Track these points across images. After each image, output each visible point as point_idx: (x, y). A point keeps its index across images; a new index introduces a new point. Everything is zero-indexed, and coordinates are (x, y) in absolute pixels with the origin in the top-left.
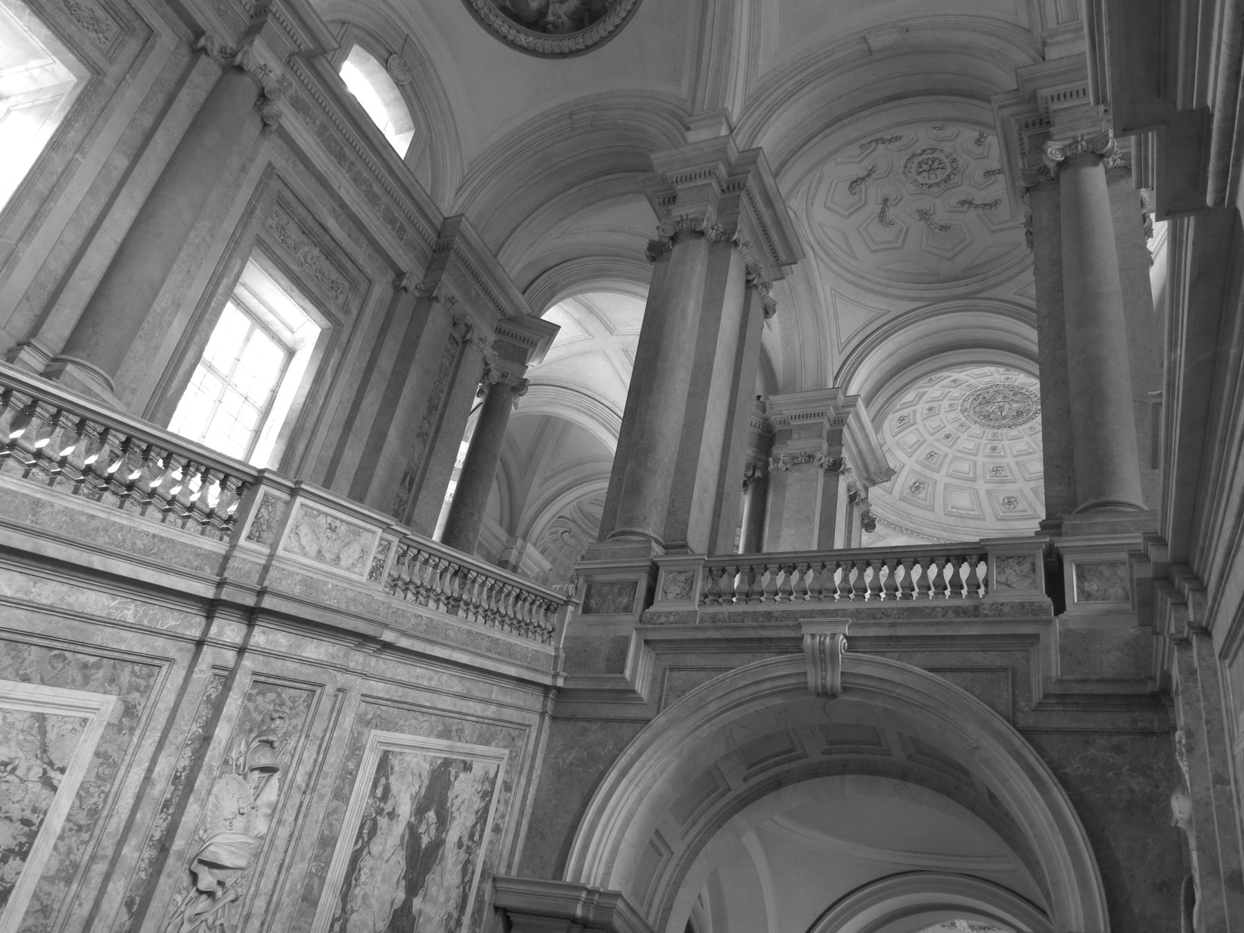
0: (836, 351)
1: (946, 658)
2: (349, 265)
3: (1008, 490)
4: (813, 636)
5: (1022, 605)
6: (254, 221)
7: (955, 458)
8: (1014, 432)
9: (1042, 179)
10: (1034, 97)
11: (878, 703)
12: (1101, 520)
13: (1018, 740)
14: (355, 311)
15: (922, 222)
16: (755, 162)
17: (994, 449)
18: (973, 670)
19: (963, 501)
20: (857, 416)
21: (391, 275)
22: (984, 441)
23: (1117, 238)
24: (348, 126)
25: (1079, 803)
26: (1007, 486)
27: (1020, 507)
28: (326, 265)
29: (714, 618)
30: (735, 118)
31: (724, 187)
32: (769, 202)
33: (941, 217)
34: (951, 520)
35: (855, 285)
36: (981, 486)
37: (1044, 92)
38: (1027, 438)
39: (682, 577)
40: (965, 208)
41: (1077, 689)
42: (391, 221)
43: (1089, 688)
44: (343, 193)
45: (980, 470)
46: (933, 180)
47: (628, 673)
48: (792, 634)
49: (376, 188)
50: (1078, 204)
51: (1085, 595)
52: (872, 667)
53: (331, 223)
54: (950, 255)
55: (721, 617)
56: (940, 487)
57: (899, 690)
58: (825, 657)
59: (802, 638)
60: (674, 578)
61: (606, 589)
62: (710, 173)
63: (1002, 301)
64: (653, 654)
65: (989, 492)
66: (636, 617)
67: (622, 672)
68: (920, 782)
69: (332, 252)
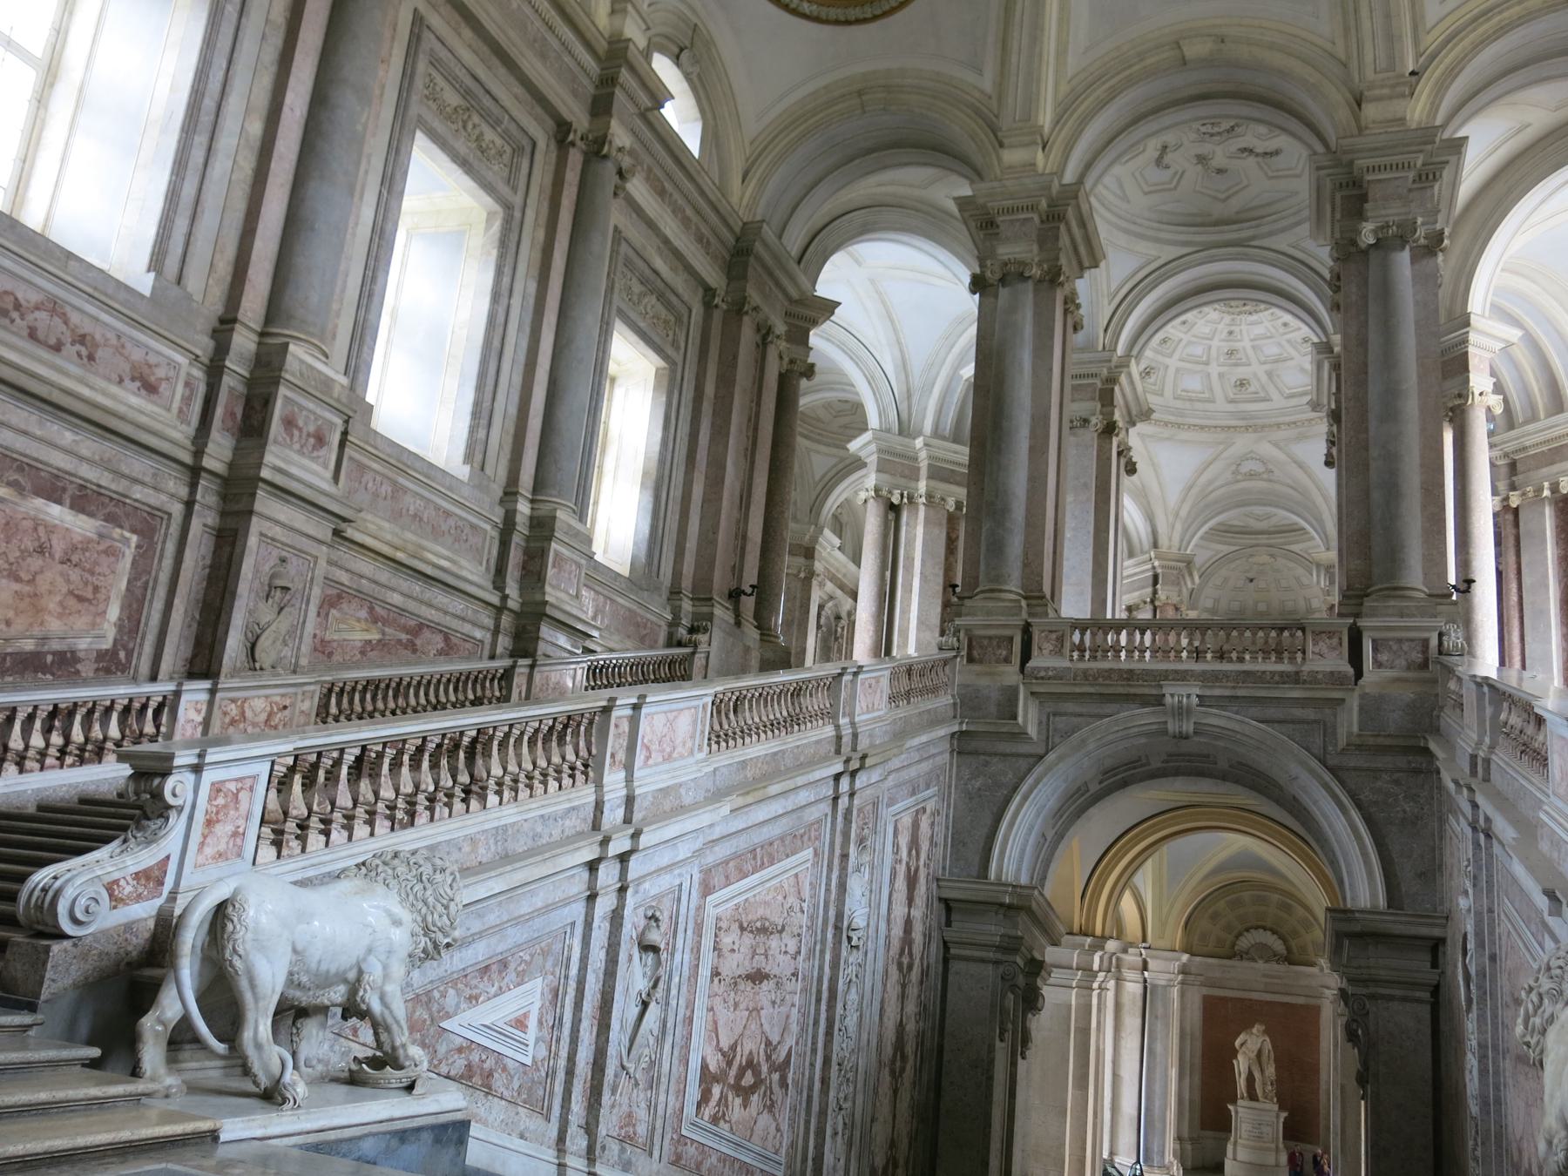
0: (1106, 302)
1: (1272, 712)
2: (674, 299)
3: (1241, 372)
4: (1172, 695)
5: (1332, 673)
6: (616, 297)
7: (1189, 343)
8: (1255, 317)
9: (1353, 249)
10: (1351, 163)
11: (1221, 743)
12: (1392, 603)
13: (1327, 777)
14: (683, 345)
16: (1076, 197)
17: (1231, 333)
18: (1293, 722)
19: (1194, 384)
20: (1130, 375)
21: (701, 291)
22: (1221, 326)
23: (1417, 323)
24: (669, 162)
25: (1369, 820)
26: (1240, 369)
27: (1252, 389)
28: (659, 306)
29: (1085, 672)
30: (1046, 130)
32: (1083, 224)
33: (1219, 160)
34: (1179, 404)
35: (1126, 231)
36: (1214, 370)
37: (1361, 163)
39: (1054, 636)
41: (1371, 741)
42: (700, 239)
43: (1380, 741)
44: (668, 232)
45: (1214, 352)
46: (1216, 129)
47: (1020, 720)
48: (1154, 692)
49: (689, 212)
50: (1387, 291)
51: (1378, 664)
52: (1217, 719)
53: (659, 264)
54: (1223, 196)
56: (1171, 371)
58: (1181, 712)
61: (986, 642)
62: (1033, 208)
65: (1221, 375)
67: (1015, 718)
68: (1237, 782)
69: (663, 292)
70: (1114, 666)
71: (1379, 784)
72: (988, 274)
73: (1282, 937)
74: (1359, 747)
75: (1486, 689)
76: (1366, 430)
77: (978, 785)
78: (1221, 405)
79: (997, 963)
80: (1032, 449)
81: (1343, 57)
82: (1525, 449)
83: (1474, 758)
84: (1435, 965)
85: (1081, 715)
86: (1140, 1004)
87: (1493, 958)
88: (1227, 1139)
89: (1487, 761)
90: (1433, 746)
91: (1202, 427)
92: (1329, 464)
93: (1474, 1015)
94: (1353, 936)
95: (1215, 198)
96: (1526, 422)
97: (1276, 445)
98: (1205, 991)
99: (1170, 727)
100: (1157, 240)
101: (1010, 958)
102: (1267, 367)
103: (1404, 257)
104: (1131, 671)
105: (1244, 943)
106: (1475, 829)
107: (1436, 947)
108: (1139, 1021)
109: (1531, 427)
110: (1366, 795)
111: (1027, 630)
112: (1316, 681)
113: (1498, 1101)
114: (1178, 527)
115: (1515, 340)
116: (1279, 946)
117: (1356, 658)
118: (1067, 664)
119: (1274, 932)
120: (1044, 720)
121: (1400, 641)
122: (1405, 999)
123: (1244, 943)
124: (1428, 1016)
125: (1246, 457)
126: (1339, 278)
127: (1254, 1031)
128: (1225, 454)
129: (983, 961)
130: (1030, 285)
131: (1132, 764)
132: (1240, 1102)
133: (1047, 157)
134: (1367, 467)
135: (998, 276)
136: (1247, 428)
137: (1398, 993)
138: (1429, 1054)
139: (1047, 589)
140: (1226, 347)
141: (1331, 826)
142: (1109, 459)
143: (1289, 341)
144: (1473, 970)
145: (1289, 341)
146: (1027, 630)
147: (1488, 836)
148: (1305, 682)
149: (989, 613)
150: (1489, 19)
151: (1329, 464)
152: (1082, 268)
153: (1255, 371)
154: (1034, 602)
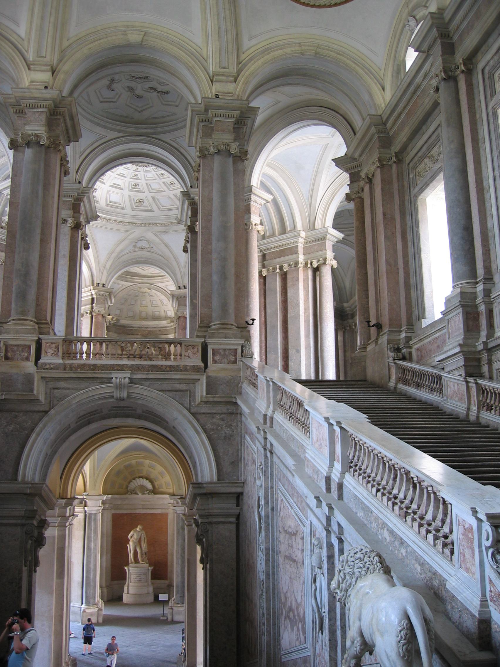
0: (78, 156)
1: (165, 386)
3: (139, 196)
4: (116, 378)
12: (221, 331)
13: (191, 418)
15: (129, 93)
16: (70, 105)
18: (176, 391)
22: (131, 171)
25: (210, 438)
31: (52, 113)
32: (72, 118)
33: (139, 92)
38: (153, 172)
40: (151, 91)
41: (211, 400)
47: (35, 392)
51: (215, 362)
52: (139, 390)
54: (140, 109)
55: (73, 365)
57: (149, 399)
58: (120, 387)
59: (112, 378)
60: (50, 346)
61: (15, 348)
63: (164, 141)
64: (45, 382)
65: (130, 196)
66: (33, 363)
67: (32, 391)
70: (87, 362)
71: (214, 420)
72: (20, 140)
73: (151, 481)
74: (206, 403)
75: (271, 383)
76: (211, 244)
77: (11, 428)
78: (129, 211)
79: (23, 525)
80: (42, 240)
81: (205, 57)
82: (269, 249)
83: (265, 416)
84: (238, 505)
85: (69, 389)
86: (83, 524)
87: (273, 509)
88: (124, 584)
89: (272, 418)
90: (239, 402)
91: (119, 222)
92: (185, 251)
93: (263, 533)
94: (201, 495)
95: (136, 110)
96: (270, 236)
97: (155, 234)
98: (114, 512)
99: (114, 394)
100: (105, 127)
101: (30, 522)
102: (153, 194)
103: (231, 160)
104: (95, 365)
105: (132, 485)
106: (265, 449)
107: (239, 497)
108: (82, 533)
109: (272, 239)
110: (209, 426)
111: (39, 343)
112: (187, 370)
113: (274, 574)
114: (105, 273)
115: (270, 200)
116: (149, 486)
117: (205, 359)
118: (61, 361)
119: (147, 479)
120: (48, 391)
121: (225, 350)
122: (224, 523)
123: (132, 485)
124: (235, 529)
125: (140, 239)
126: (199, 166)
127: (138, 529)
128: (130, 237)
129: (15, 525)
130: (43, 149)
131: (93, 413)
132: (131, 565)
133: (54, 79)
134: (210, 262)
135: (25, 142)
136: (141, 224)
137: (222, 520)
138: (235, 548)
139: (49, 319)
140: (134, 182)
141: (192, 442)
142: (77, 242)
143: (163, 183)
144: (263, 514)
145: (163, 183)
146: (39, 343)
147: (271, 453)
148: (181, 371)
149: (17, 332)
150: (269, 53)
151: (185, 251)
152: (69, 141)
153: (146, 195)
154: (42, 326)
